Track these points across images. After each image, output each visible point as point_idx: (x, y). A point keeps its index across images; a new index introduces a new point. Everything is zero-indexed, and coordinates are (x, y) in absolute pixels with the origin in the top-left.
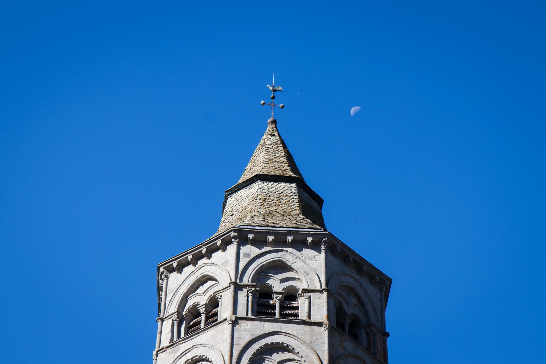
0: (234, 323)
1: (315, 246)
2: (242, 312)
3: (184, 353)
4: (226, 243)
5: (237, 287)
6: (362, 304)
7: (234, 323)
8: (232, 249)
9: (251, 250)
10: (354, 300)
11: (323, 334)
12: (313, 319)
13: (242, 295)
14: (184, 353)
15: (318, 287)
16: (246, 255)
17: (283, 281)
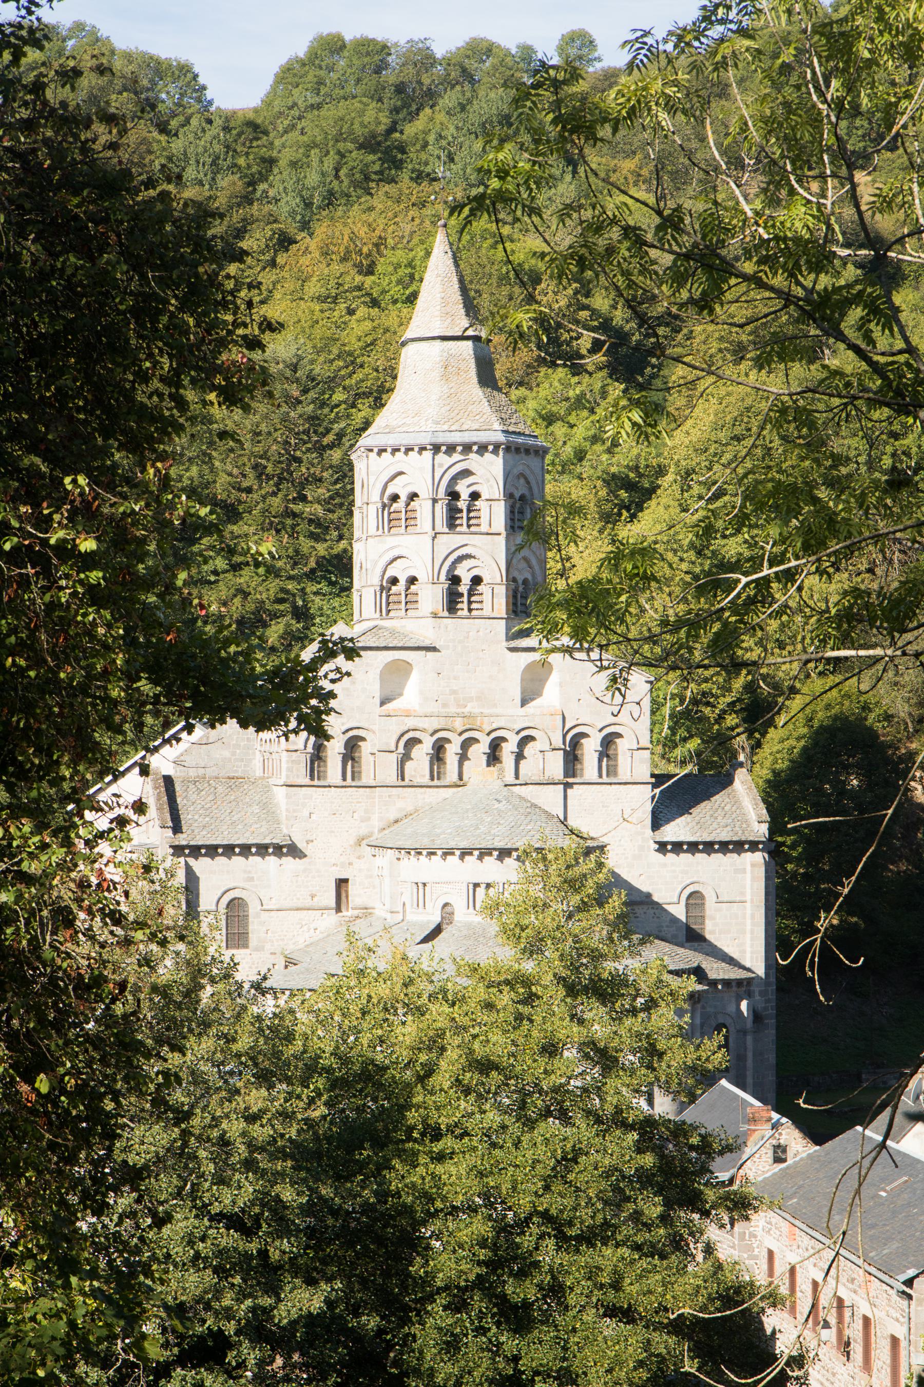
0: (434, 538)
1: (495, 451)
2: (439, 528)
3: (392, 548)
4: (422, 449)
5: (435, 501)
6: (528, 482)
7: (434, 538)
8: (428, 455)
9: (442, 458)
10: (522, 481)
11: (501, 541)
12: (493, 531)
13: (438, 506)
14: (392, 548)
15: (497, 497)
16: (441, 465)
17: (468, 486)
